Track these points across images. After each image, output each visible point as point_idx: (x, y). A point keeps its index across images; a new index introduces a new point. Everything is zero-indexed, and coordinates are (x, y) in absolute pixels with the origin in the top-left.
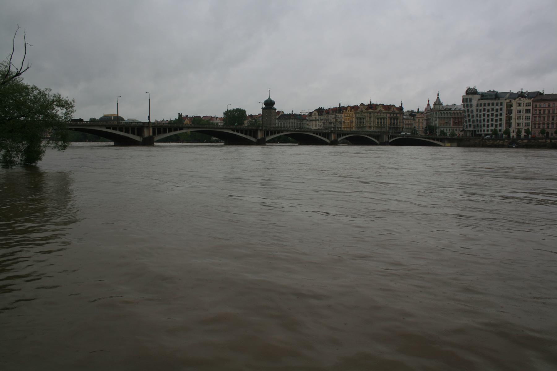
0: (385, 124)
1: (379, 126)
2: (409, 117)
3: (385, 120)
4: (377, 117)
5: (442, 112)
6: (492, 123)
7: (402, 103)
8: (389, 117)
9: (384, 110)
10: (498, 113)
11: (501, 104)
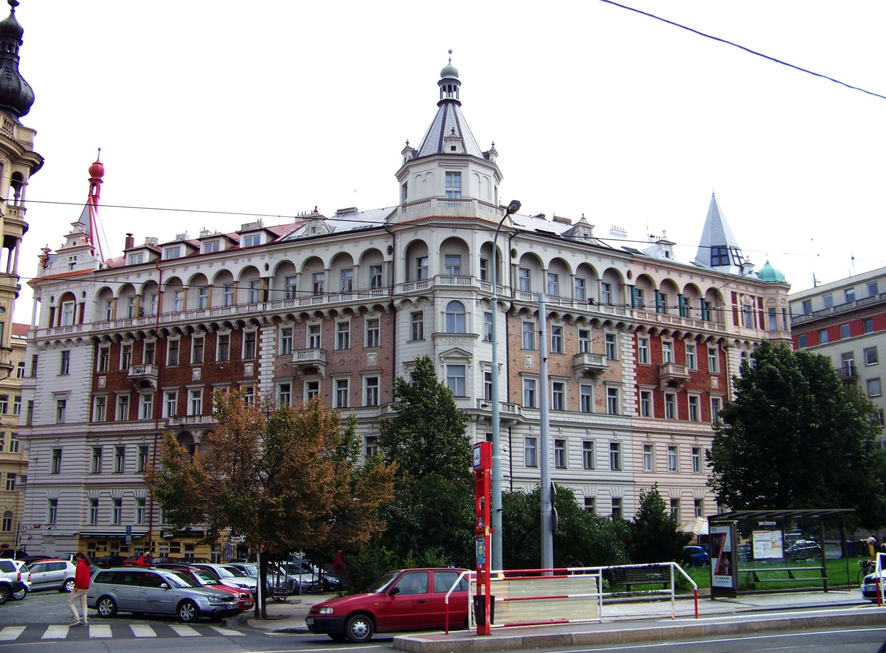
5: (547, 255)
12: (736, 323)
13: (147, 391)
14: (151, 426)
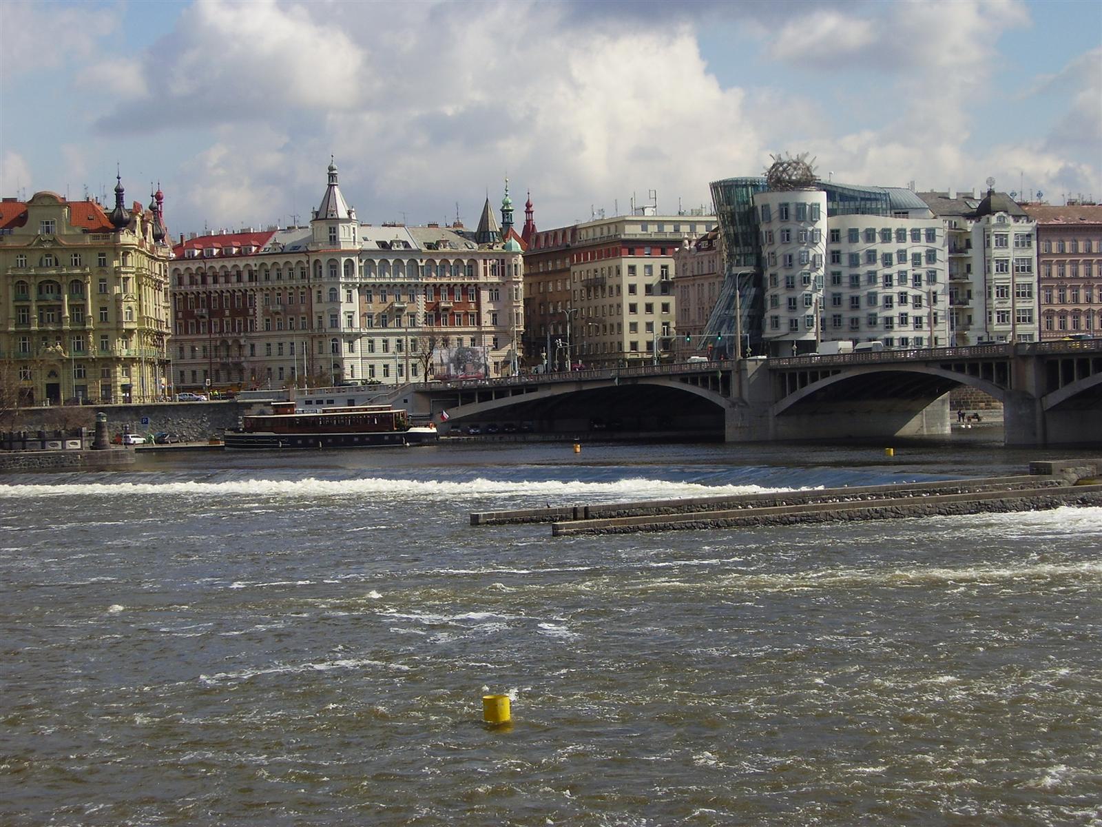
6: (904, 309)
10: (922, 271)
11: (931, 235)
12: (486, 275)
13: (204, 320)
14: (208, 336)
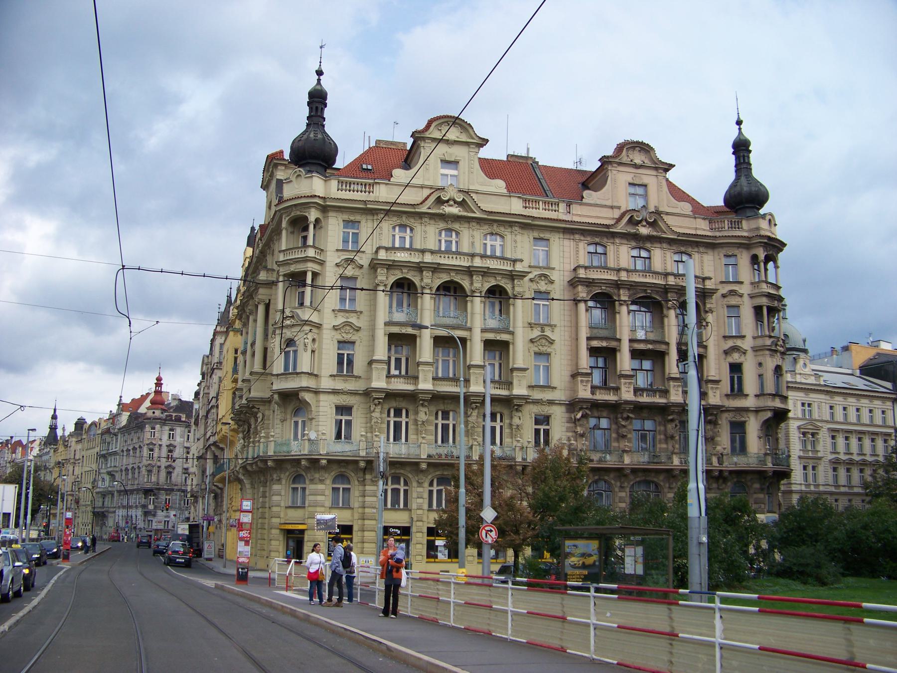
0: (520, 355)
1: (426, 385)
2: (860, 383)
3: (521, 311)
4: (391, 266)
7: (747, 134)
8: (573, 283)
9: (499, 185)
